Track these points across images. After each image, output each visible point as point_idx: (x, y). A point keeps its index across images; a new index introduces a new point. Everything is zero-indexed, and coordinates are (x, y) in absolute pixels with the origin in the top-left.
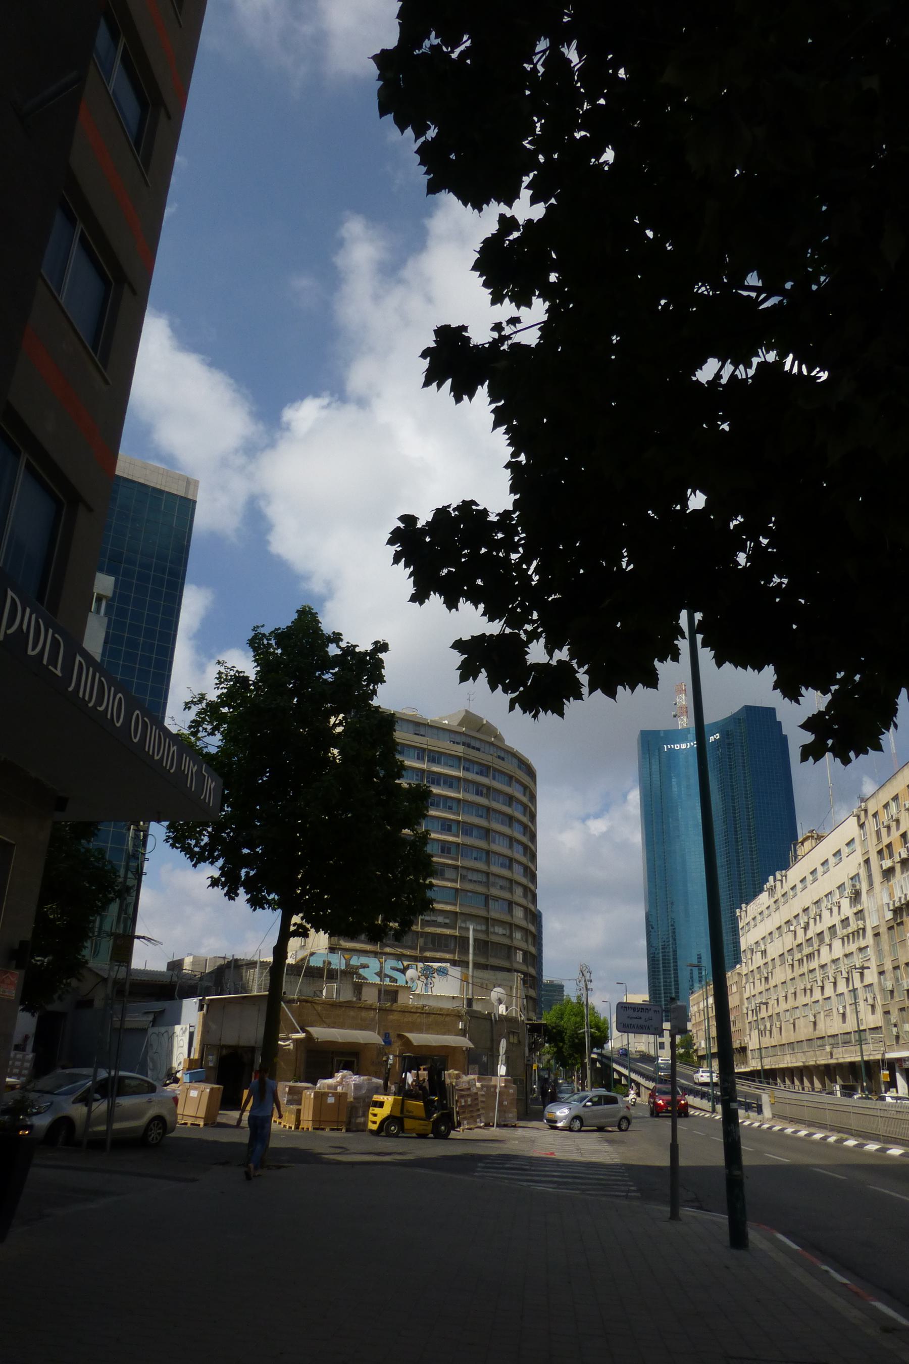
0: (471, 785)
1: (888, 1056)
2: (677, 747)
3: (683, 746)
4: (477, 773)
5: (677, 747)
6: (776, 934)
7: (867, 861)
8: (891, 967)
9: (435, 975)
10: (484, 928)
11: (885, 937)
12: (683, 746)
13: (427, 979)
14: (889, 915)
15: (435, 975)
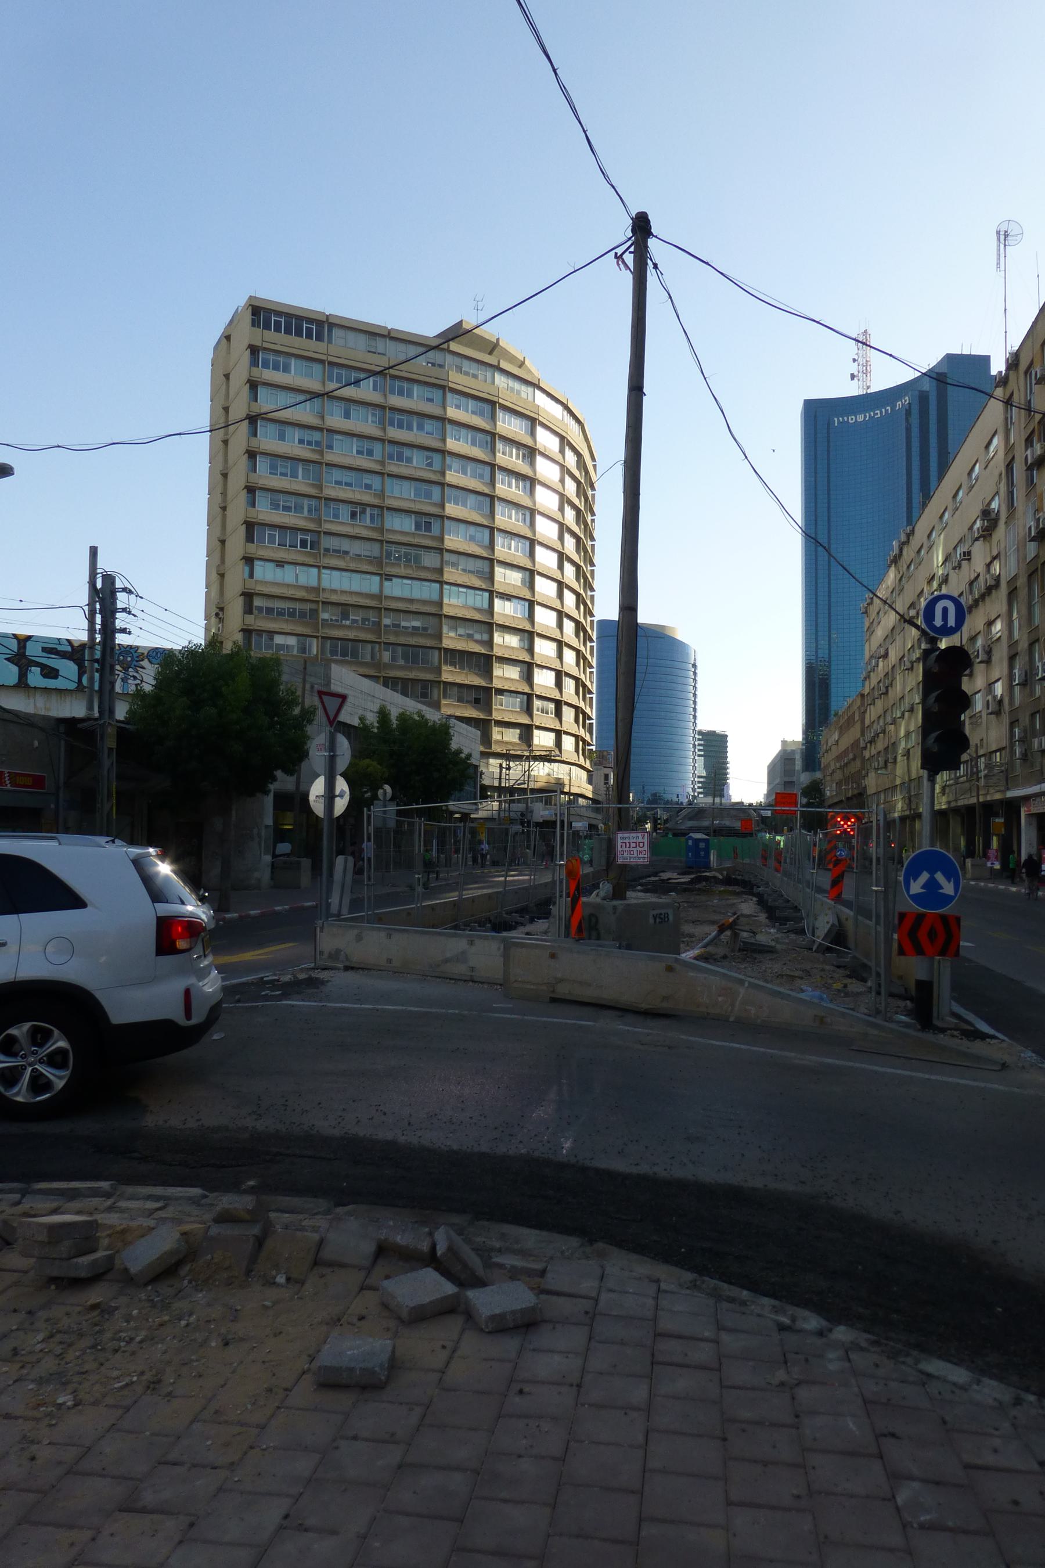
0: (463, 431)
1: (1011, 794)
2: (852, 419)
3: (860, 418)
4: (473, 412)
5: (852, 419)
6: (898, 630)
7: (1009, 467)
8: (1026, 645)
9: (145, 663)
10: (485, 637)
11: (1023, 593)
12: (860, 418)
13: (126, 669)
14: (1032, 548)
15: (145, 663)
